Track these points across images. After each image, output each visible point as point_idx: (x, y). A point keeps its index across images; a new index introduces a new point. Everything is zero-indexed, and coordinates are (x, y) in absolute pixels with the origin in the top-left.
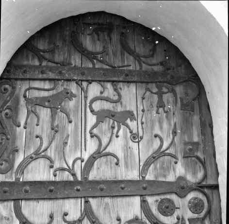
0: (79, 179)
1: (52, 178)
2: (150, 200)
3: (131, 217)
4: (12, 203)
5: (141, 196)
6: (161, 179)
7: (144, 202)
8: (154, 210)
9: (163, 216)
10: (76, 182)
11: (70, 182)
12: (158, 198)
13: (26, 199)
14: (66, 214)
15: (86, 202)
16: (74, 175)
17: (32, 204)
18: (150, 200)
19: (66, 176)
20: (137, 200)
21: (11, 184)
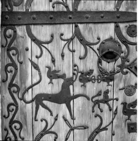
0: (71, 10)
1: (52, 9)
2: (122, 26)
3: (107, 37)
4: (25, 27)
5: (115, 23)
6: (130, 11)
7: (117, 27)
8: (124, 33)
9: (130, 37)
10: (69, 12)
11: (65, 12)
12: (128, 24)
13: (34, 24)
14: (62, 35)
15: (76, 26)
16: (67, 7)
17: (39, 27)
18: (122, 26)
19: (62, 8)
20: (112, 26)
21: (23, 13)
